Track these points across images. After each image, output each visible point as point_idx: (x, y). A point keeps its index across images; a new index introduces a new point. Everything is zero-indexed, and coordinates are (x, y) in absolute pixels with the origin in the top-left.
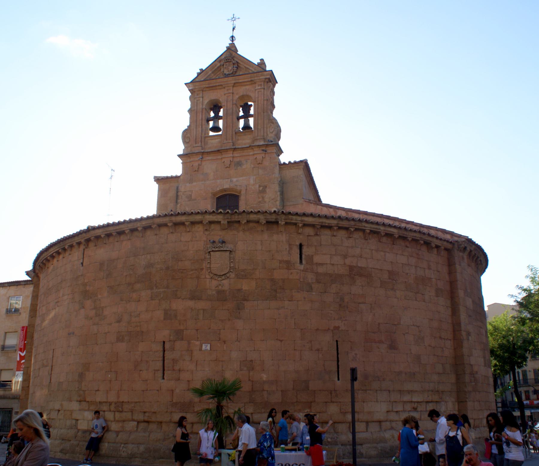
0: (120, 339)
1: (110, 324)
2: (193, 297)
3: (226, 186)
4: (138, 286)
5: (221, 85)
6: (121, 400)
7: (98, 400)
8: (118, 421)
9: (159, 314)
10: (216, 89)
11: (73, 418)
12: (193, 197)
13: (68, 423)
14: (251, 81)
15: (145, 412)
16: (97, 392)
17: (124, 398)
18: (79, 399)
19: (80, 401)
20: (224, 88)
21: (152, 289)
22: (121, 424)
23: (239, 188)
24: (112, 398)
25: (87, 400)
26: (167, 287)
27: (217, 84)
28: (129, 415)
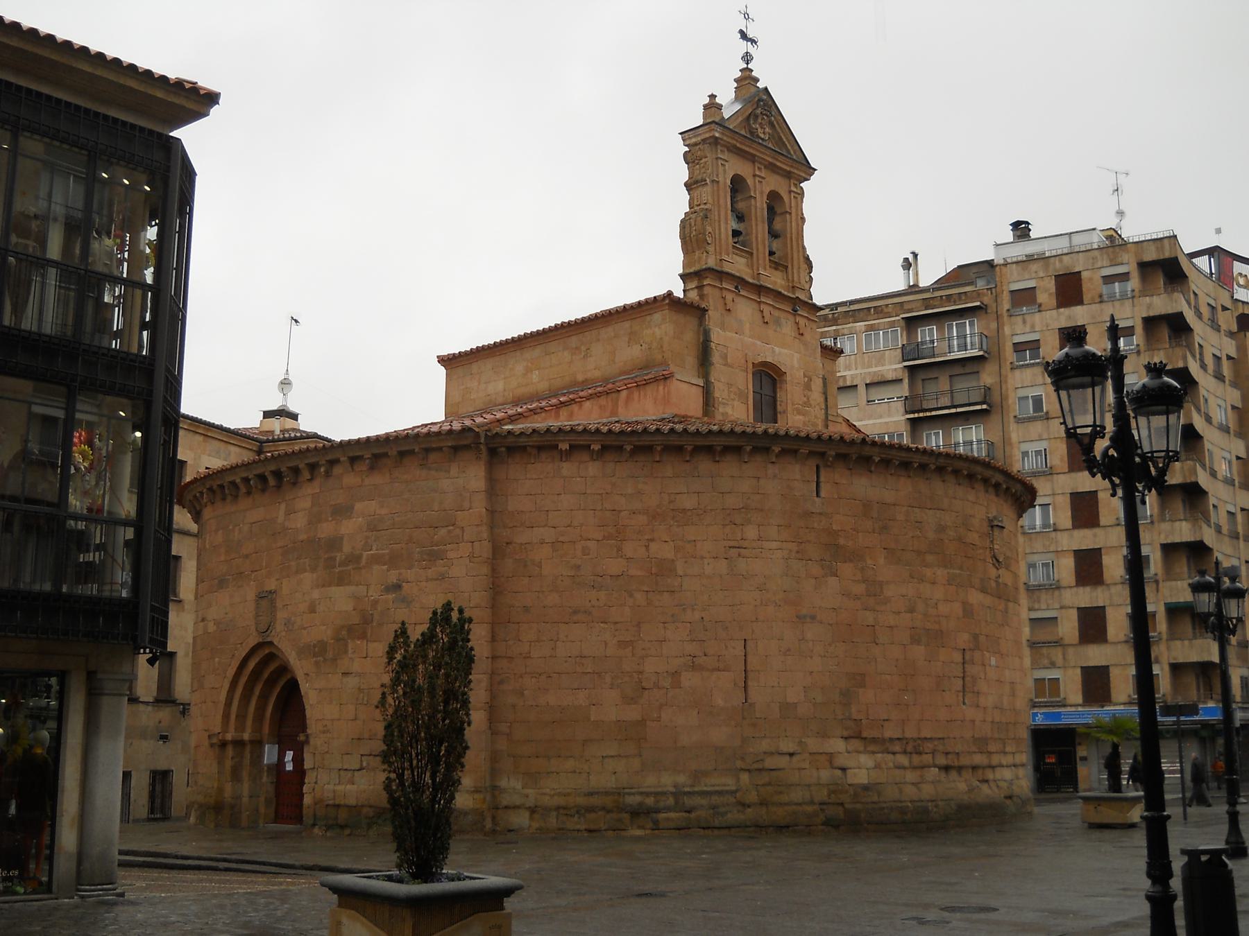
0: (915, 640)
2: (983, 590)
4: (930, 558)
5: (754, 156)
6: (923, 735)
7: (888, 734)
8: (915, 768)
9: (957, 608)
10: (744, 157)
11: (836, 765)
14: (790, 172)
16: (886, 724)
17: (926, 733)
18: (845, 734)
20: (754, 162)
21: (946, 567)
22: (918, 772)
25: (864, 735)
26: (961, 568)
27: (752, 151)
28: (927, 759)
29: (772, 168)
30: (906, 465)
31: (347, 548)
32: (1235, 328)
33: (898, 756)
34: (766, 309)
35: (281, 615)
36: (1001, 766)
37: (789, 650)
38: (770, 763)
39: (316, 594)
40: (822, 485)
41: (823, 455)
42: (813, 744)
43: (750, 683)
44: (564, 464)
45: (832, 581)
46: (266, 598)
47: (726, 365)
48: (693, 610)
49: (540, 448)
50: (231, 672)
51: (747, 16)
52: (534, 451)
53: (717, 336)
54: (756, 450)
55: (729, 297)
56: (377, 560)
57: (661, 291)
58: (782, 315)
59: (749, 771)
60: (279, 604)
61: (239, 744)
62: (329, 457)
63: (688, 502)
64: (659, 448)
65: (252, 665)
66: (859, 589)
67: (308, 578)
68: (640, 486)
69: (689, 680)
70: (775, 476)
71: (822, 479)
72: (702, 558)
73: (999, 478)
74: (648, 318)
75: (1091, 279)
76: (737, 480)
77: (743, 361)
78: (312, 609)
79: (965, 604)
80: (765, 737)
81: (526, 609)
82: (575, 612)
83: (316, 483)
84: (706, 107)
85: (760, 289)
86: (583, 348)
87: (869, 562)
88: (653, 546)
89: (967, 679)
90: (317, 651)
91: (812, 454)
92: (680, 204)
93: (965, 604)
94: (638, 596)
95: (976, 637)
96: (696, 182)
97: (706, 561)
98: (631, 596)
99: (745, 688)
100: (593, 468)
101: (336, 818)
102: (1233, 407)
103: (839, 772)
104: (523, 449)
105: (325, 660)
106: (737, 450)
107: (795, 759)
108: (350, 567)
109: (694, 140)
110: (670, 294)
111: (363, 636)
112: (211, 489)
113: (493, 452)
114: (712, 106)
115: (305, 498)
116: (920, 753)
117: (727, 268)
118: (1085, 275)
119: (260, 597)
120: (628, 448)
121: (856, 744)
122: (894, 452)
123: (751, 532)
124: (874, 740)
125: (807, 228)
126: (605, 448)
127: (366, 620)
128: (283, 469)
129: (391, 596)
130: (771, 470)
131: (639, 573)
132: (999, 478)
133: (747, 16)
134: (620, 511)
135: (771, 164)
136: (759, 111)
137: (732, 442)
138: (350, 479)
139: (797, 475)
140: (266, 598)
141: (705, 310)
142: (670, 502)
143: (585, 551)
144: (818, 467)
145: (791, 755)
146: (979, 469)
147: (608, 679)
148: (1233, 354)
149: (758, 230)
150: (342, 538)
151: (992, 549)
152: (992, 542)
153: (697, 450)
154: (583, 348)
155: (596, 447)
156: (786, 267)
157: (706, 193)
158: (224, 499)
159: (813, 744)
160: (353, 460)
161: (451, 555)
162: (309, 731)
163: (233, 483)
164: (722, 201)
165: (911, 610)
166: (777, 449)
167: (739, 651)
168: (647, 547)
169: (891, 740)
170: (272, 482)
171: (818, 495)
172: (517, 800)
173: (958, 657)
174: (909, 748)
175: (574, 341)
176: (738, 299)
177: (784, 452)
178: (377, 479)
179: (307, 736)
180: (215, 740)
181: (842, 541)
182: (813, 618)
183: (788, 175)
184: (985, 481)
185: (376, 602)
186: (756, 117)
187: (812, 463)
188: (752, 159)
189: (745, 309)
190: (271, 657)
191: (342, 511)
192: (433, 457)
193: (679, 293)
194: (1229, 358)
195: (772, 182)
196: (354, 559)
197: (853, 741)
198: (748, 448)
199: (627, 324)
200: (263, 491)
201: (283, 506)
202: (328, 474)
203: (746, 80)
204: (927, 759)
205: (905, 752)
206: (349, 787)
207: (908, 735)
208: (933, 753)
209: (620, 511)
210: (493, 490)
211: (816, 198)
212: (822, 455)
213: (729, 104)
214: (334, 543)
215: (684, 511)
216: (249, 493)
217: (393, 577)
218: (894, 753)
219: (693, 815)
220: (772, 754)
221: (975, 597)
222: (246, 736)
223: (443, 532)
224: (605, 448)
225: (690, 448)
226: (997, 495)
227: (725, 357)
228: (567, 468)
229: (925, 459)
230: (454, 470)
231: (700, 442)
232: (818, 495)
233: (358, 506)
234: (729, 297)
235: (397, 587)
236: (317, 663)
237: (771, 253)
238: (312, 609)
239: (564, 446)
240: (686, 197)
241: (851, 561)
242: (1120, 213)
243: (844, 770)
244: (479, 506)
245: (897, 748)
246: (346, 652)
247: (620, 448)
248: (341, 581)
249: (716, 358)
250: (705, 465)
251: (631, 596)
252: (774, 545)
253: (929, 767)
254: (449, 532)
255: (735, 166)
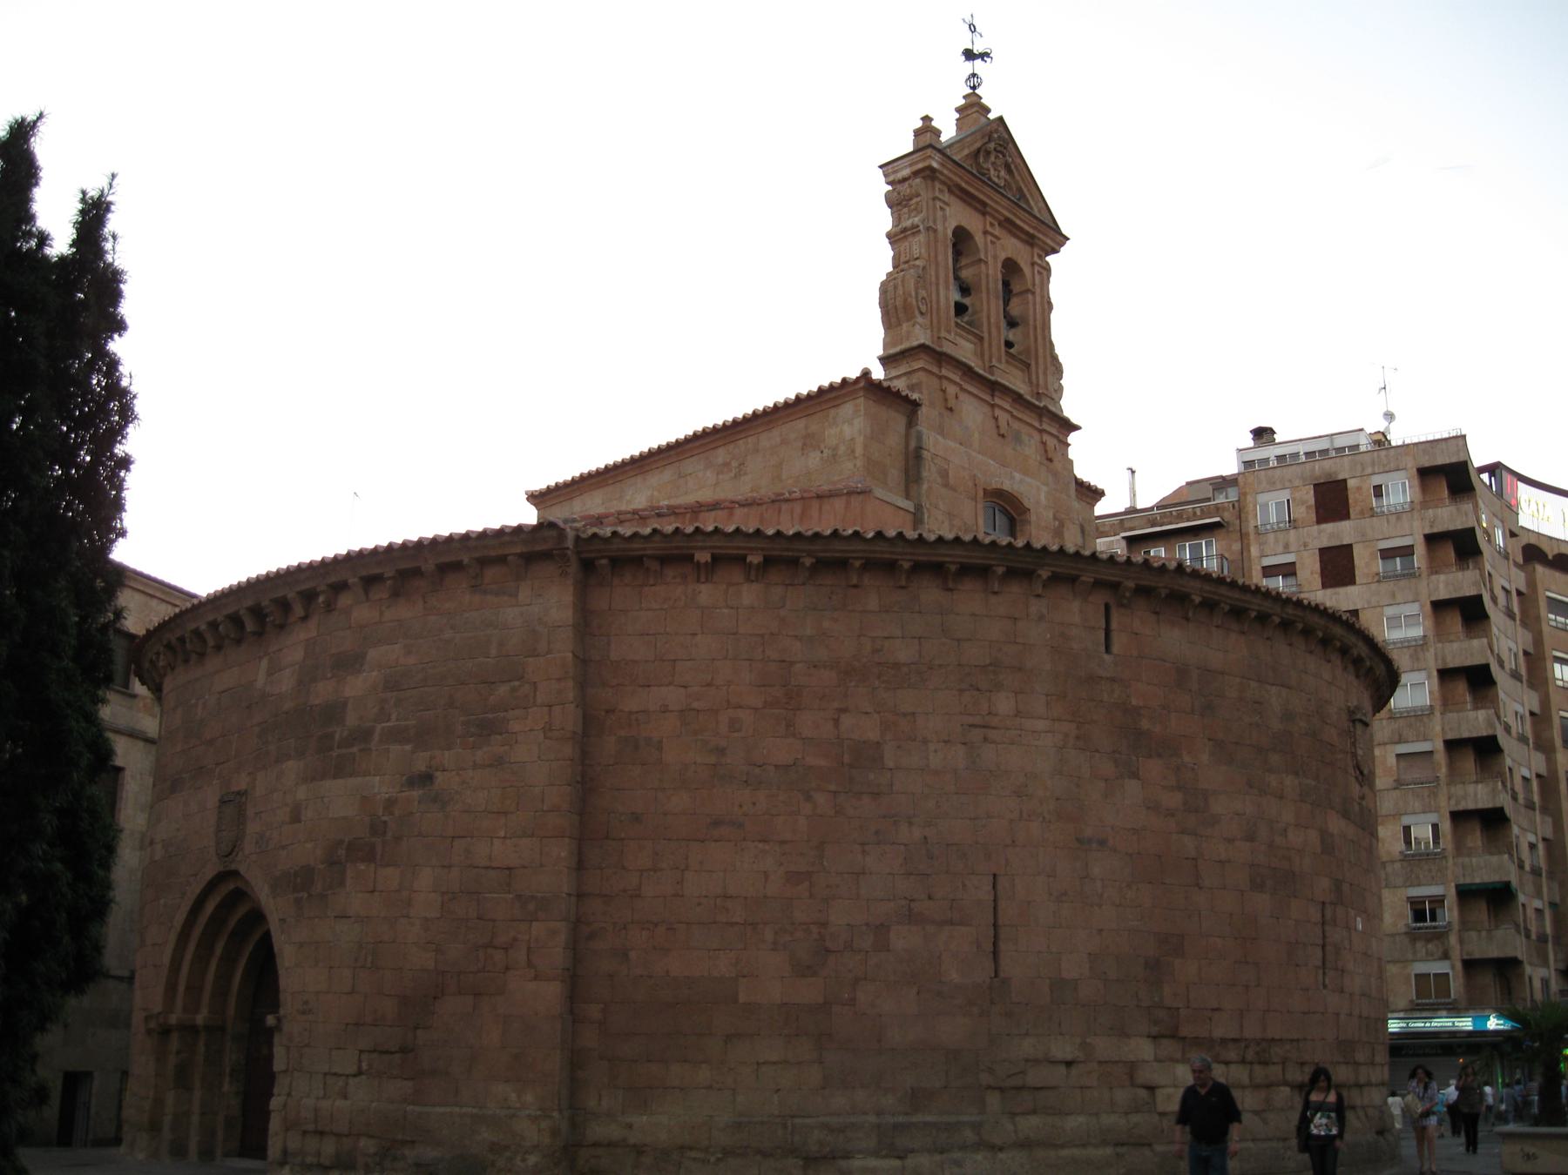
1: (1230, 841)
2: (1345, 815)
3: (1007, 486)
5: (984, 204)
7: (1218, 1033)
8: (1257, 1087)
9: (1313, 836)
10: (970, 205)
12: (952, 481)
13: (1122, 1096)
14: (1033, 237)
15: (1302, 1064)
18: (1155, 1030)
19: (1155, 1037)
20: (984, 214)
23: (1026, 503)
24: (1252, 1031)
25: (1185, 1031)
27: (981, 197)
28: (1275, 1071)
29: (1008, 225)
30: (1238, 613)
31: (351, 719)
32: (1520, 560)
33: (1233, 1067)
34: (1004, 418)
35: (252, 828)
36: (1369, 1084)
37: (1065, 894)
38: (1034, 1077)
39: (302, 793)
40: (1115, 637)
41: (1115, 587)
42: (1104, 1046)
43: (1002, 946)
44: (703, 587)
45: (1132, 786)
46: (234, 804)
47: (946, 485)
48: (911, 824)
49: (664, 560)
50: (180, 918)
51: (972, 28)
52: (655, 566)
53: (933, 442)
54: (1012, 574)
55: (952, 390)
56: (397, 735)
57: (854, 374)
58: (1025, 429)
59: (1001, 1090)
60: (250, 812)
61: (189, 1029)
62: (333, 579)
63: (904, 653)
64: (857, 564)
65: (210, 907)
66: (1174, 800)
67: (292, 767)
68: (826, 624)
69: (903, 939)
70: (1041, 618)
71: (1114, 625)
72: (925, 741)
73: (1362, 649)
74: (832, 411)
75: (1359, 489)
76: (982, 618)
77: (970, 484)
78: (296, 818)
79: (1324, 834)
80: (1027, 1034)
81: (636, 818)
82: (717, 823)
83: (313, 624)
84: (917, 133)
85: (994, 387)
86: (734, 464)
87: (1187, 759)
88: (847, 721)
89: (1328, 948)
90: (300, 882)
91: (1098, 584)
92: (881, 260)
93: (1324, 834)
94: (821, 798)
95: (1338, 885)
96: (904, 230)
97: (932, 747)
98: (809, 798)
99: (995, 953)
100: (749, 594)
101: (319, 1154)
102: (1526, 653)
103: (1143, 1093)
104: (637, 561)
105: (310, 896)
106: (983, 572)
107: (1074, 1071)
108: (355, 749)
109: (900, 175)
110: (866, 374)
111: (370, 857)
112: (169, 646)
113: (588, 566)
114: (926, 130)
115: (293, 647)
116: (1265, 1063)
117: (947, 348)
118: (1351, 483)
119: (223, 802)
120: (808, 561)
121: (1169, 1047)
122: (1223, 590)
123: (1004, 704)
124: (1197, 1042)
125: (1055, 317)
126: (769, 562)
127: (377, 828)
128: (265, 603)
129: (416, 793)
130: (1036, 607)
131: (823, 763)
132: (1362, 649)
133: (972, 28)
134: (792, 663)
135: (1008, 220)
136: (992, 146)
137: (977, 558)
138: (363, 613)
139: (1075, 614)
140: (234, 804)
141: (916, 405)
142: (875, 651)
143: (734, 725)
144: (1107, 607)
145: (1069, 1064)
146: (1338, 630)
147: (769, 935)
148: (1523, 589)
149: (989, 306)
150: (345, 704)
151: (1354, 755)
152: (1354, 744)
153: (918, 568)
154: (734, 464)
155: (755, 559)
156: (1028, 366)
157: (917, 245)
158: (186, 661)
159: (1104, 1046)
160: (370, 582)
161: (515, 726)
162: (282, 1012)
163: (197, 633)
164: (940, 258)
165: (1251, 838)
166: (1045, 573)
167: (985, 894)
168: (836, 721)
169: (1224, 1041)
170: (250, 626)
171: (1108, 649)
172: (613, 1131)
173: (1315, 915)
174: (1250, 1055)
175: (721, 455)
176: (963, 396)
177: (1055, 579)
178: (405, 611)
179: (279, 1020)
180: (152, 1025)
181: (1145, 724)
182: (1102, 843)
183: (1030, 240)
184: (1344, 651)
185: (390, 803)
186: (988, 153)
187: (1100, 598)
188: (982, 208)
189: (972, 412)
190: (239, 895)
191: (349, 663)
192: (491, 573)
193: (878, 373)
194: (1519, 593)
195: (1011, 247)
196: (362, 736)
197: (1165, 1042)
198: (1000, 570)
199: (800, 424)
200: (239, 642)
201: (264, 663)
202: (329, 607)
203: (972, 107)
204: (1275, 1071)
205: (1243, 1061)
206: (340, 1103)
207: (1248, 1034)
208: (1284, 1062)
209: (792, 663)
210: (586, 623)
211: (1067, 275)
212: (1115, 587)
213: (948, 130)
214: (333, 713)
215: (897, 666)
216: (219, 648)
217: (420, 766)
218: (1227, 1063)
219: (910, 1162)
220: (1037, 1061)
221: (1336, 825)
222: (200, 1019)
223: (503, 690)
224: (769, 562)
225: (906, 565)
226: (1357, 677)
227: (944, 474)
228: (707, 593)
229: (1267, 606)
230: (524, 593)
231: (923, 555)
232: (1108, 649)
233: (372, 654)
234: (952, 390)
235: (426, 778)
236: (298, 901)
237: (1009, 344)
238: (296, 818)
239: (703, 557)
240: (888, 253)
241: (1160, 756)
242: (1390, 416)
243: (1151, 1089)
244: (564, 648)
245: (1232, 1055)
246: (342, 883)
247: (794, 562)
248: (340, 770)
249: (929, 472)
250: (930, 593)
251: (809, 798)
252: (1041, 725)
253: (1278, 1085)
254: (513, 690)
255: (958, 214)
